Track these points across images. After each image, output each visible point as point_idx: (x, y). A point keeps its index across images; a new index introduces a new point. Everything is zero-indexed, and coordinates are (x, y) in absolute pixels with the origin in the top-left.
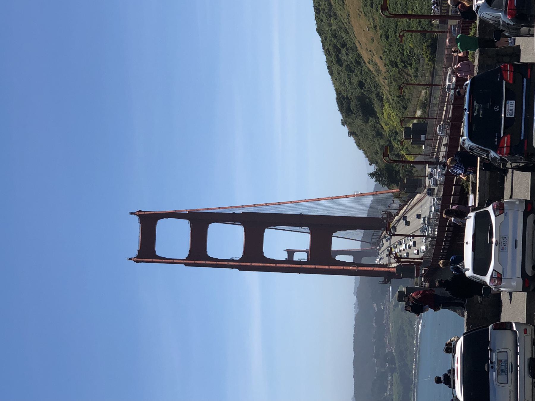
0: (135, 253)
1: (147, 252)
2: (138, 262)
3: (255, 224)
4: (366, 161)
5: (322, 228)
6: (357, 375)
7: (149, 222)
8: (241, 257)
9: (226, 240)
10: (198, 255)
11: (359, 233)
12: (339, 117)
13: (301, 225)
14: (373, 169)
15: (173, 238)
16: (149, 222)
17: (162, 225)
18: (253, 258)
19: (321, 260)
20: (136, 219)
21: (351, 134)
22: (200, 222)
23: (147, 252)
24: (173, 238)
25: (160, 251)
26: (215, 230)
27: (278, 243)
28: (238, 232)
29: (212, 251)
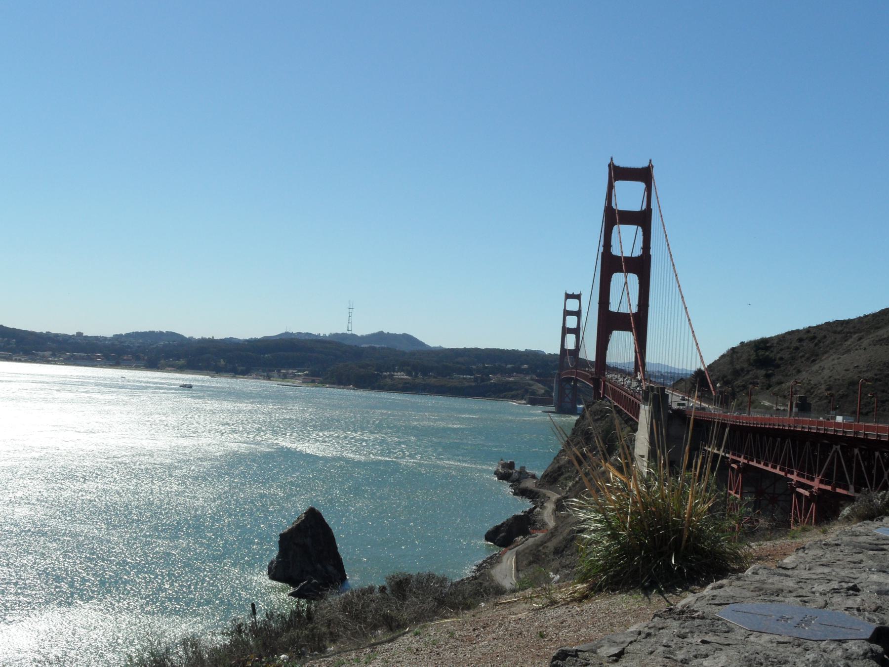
2: (609, 165)
3: (640, 266)
5: (637, 323)
6: (487, 350)
7: (644, 175)
8: (614, 253)
9: (627, 240)
10: (613, 217)
12: (746, 340)
13: (639, 305)
15: (630, 196)
17: (641, 186)
18: (610, 264)
20: (646, 164)
21: (733, 349)
22: (642, 219)
23: (618, 173)
24: (630, 196)
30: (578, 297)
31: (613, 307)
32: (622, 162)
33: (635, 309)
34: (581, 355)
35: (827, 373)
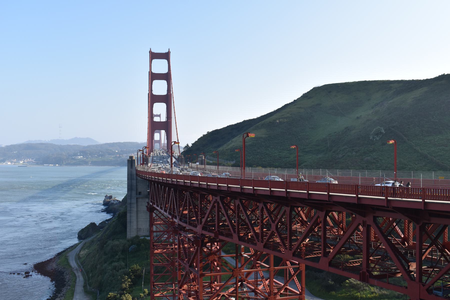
0: (153, 51)
1: (154, 56)
2: (150, 52)
3: (167, 99)
4: (193, 142)
5: (166, 126)
7: (166, 56)
9: (160, 88)
10: (153, 77)
11: (166, 142)
12: (210, 131)
14: (190, 145)
15: (160, 66)
16: (166, 56)
17: (165, 61)
18: (153, 99)
19: (154, 127)
20: (167, 51)
21: (204, 136)
22: (167, 77)
23: (154, 56)
24: (160, 66)
25: (154, 61)
26: (164, 83)
27: (160, 109)
28: (164, 92)
29: (155, 82)
30: (159, 116)
31: (156, 119)
32: (155, 51)
33: (164, 119)
34: (163, 142)
35: (233, 144)
